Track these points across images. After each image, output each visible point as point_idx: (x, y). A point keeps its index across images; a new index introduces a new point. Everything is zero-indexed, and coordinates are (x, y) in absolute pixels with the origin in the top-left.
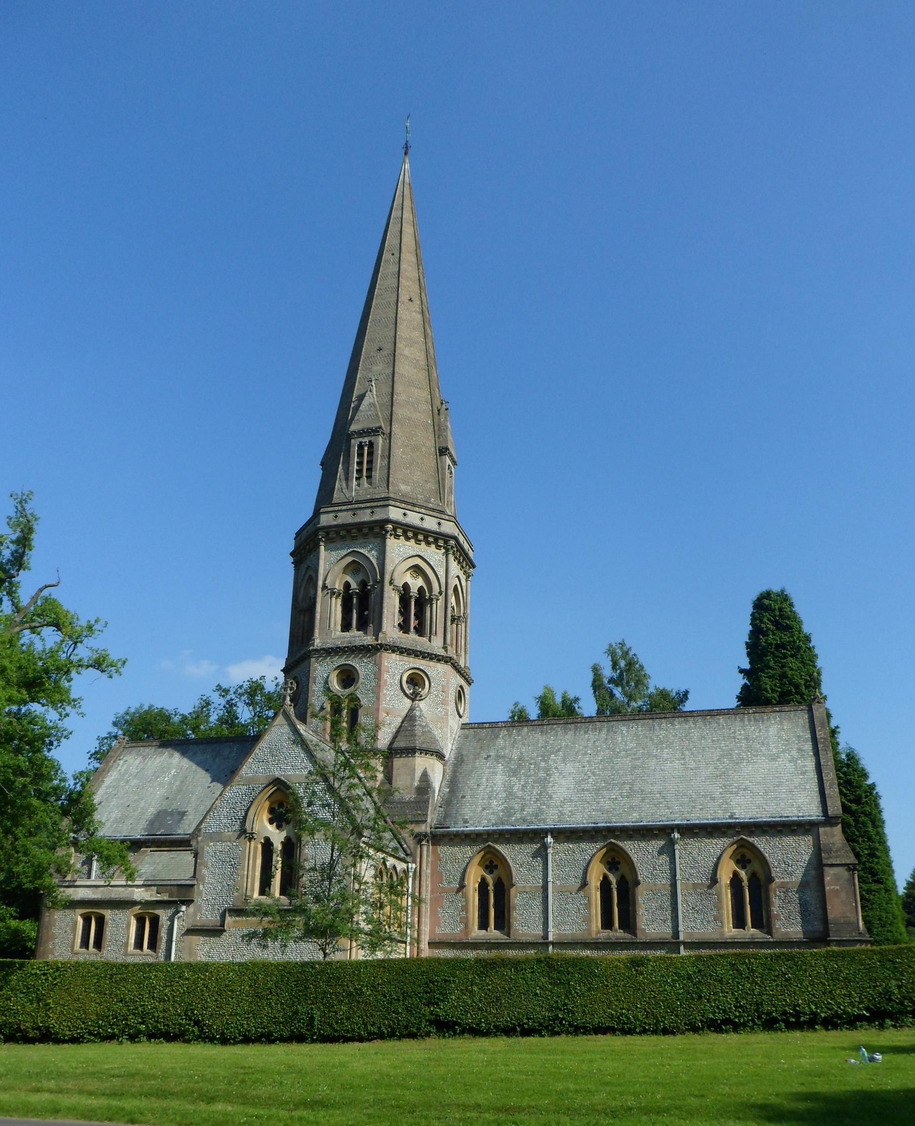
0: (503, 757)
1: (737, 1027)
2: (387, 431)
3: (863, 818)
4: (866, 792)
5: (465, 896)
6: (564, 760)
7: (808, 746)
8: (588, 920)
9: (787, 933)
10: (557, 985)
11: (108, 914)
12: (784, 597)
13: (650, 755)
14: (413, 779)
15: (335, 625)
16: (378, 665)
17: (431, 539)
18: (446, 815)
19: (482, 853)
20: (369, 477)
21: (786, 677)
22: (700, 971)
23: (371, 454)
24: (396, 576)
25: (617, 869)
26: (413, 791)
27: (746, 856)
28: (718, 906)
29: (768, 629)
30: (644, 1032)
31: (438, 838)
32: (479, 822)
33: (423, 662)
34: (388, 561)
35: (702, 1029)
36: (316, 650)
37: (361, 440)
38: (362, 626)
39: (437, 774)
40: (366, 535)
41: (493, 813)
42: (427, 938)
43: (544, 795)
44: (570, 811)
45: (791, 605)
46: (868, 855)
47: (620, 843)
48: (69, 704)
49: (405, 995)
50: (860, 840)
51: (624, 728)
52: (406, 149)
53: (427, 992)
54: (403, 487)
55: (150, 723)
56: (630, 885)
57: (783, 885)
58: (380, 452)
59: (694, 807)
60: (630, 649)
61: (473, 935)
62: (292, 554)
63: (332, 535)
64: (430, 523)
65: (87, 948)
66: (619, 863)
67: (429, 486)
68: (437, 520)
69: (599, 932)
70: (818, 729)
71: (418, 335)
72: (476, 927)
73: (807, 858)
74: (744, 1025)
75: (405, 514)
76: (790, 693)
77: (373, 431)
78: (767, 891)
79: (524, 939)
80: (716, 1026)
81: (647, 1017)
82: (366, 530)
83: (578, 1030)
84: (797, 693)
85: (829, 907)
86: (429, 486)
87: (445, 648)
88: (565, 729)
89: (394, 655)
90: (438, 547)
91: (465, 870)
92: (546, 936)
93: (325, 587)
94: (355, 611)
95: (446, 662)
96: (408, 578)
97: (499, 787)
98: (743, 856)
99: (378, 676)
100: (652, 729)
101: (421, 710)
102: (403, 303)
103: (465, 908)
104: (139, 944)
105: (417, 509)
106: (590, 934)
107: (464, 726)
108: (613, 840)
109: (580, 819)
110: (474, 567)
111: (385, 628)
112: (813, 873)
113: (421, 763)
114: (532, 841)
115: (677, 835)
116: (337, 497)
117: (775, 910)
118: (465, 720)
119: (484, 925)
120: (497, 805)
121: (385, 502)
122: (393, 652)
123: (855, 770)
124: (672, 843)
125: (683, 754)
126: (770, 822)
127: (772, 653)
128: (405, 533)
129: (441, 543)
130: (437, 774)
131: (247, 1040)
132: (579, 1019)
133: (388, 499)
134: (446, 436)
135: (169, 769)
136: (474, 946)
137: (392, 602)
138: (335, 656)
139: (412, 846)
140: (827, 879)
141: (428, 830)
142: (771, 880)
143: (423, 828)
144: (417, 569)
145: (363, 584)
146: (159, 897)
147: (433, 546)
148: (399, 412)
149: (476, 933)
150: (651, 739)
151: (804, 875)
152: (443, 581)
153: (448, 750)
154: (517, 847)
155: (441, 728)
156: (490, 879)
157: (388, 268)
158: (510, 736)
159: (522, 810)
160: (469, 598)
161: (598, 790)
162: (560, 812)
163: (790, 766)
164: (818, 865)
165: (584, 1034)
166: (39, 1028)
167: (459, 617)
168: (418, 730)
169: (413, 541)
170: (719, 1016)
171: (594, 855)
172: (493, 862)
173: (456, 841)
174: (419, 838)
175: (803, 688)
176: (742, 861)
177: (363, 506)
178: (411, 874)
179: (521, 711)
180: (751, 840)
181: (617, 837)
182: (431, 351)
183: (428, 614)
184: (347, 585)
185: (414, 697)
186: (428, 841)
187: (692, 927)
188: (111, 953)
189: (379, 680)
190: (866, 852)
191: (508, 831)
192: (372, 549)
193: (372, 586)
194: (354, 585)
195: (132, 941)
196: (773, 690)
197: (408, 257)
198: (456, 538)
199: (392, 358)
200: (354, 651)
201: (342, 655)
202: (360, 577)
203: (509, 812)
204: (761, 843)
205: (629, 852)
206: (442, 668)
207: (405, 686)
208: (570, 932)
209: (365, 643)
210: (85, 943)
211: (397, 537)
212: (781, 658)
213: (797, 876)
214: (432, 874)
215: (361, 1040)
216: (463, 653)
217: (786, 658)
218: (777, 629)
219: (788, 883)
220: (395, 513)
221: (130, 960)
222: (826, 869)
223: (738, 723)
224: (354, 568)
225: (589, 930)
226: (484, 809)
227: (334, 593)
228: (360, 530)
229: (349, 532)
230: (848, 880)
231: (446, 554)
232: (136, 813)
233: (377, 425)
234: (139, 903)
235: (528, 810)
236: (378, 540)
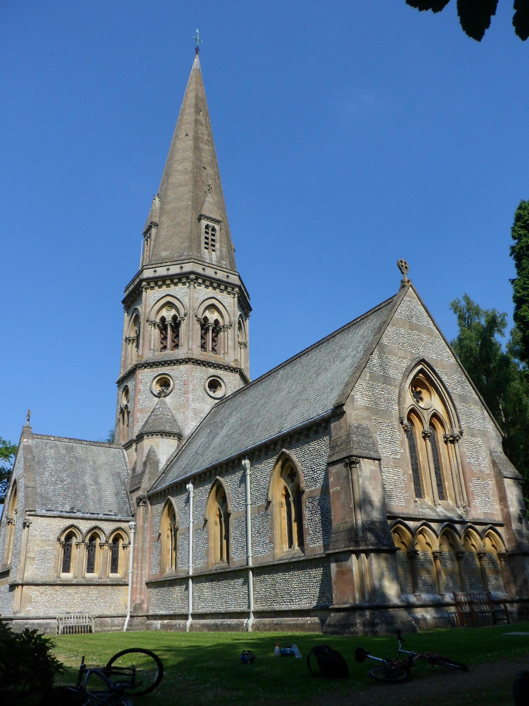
17: (176, 281)
54: (164, 254)
64: (175, 270)
68: (179, 266)
71: (190, 154)
89: (146, 370)
90: (184, 284)
95: (187, 362)
122: (145, 367)
129: (184, 280)
143: (140, 493)
144: (169, 305)
155: (183, 413)
174: (139, 500)
178: (133, 531)
186: (144, 502)
198: (192, 273)
206: (183, 368)
207: (157, 389)
211: (152, 288)
230: (347, 476)
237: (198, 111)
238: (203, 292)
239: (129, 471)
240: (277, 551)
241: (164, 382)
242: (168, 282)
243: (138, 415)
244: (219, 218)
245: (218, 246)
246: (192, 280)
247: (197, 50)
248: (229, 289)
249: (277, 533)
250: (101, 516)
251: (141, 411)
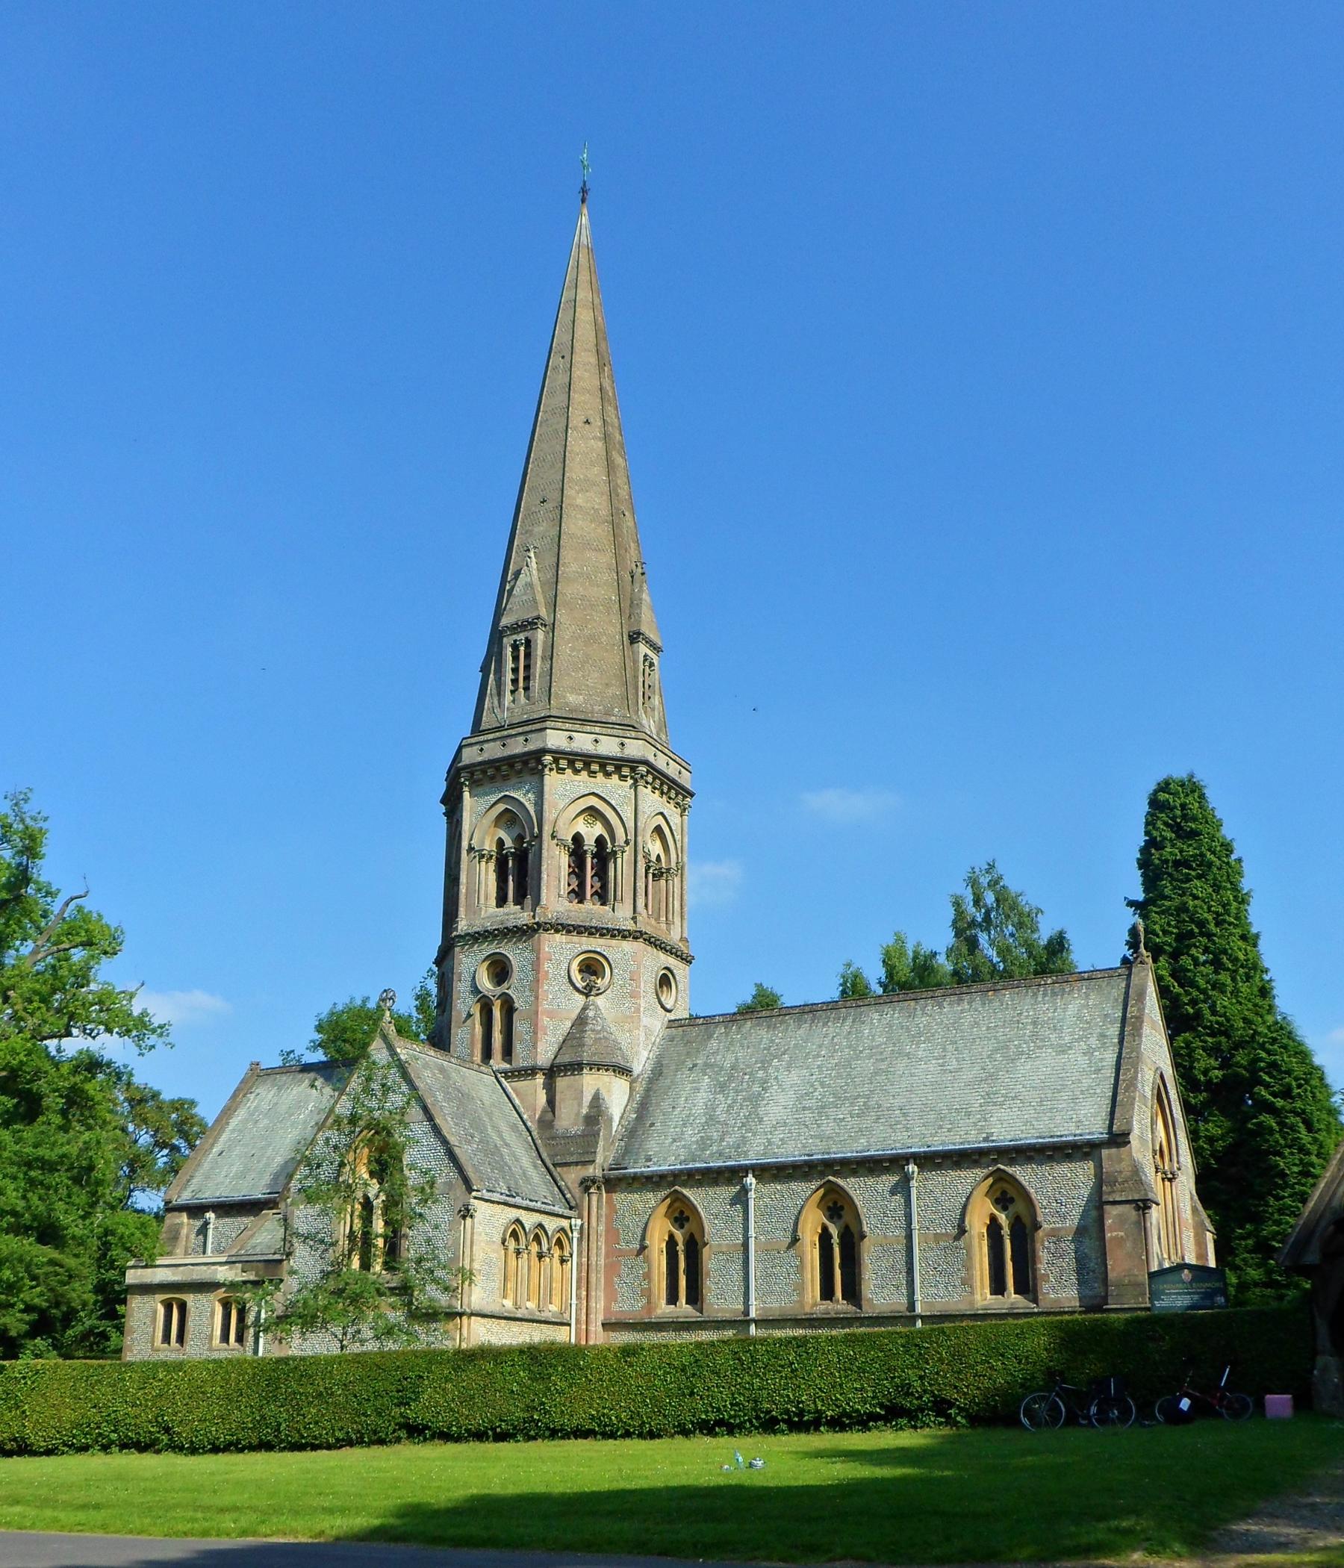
0: (712, 1066)
1: (731, 1429)
2: (549, 620)
3: (1292, 1119)
4: (1296, 1079)
5: (647, 1260)
6: (788, 1068)
7: (1114, 1031)
8: (800, 1288)
9: (1057, 1300)
10: (537, 1380)
11: (190, 1299)
12: (1192, 787)
13: (901, 1053)
14: (580, 1105)
15: (486, 898)
16: (537, 951)
17: (610, 768)
18: (627, 1151)
19: (668, 1201)
20: (526, 689)
21: (1187, 910)
22: (696, 1361)
23: (528, 655)
24: (560, 823)
25: (840, 1217)
26: (581, 1120)
27: (1007, 1193)
28: (968, 1267)
29: (1164, 838)
30: (628, 1435)
31: (614, 1183)
32: (665, 1159)
33: (601, 941)
34: (546, 807)
35: (694, 1433)
36: (460, 936)
37: (515, 637)
38: (519, 900)
39: (617, 1096)
40: (520, 772)
41: (684, 1147)
42: (601, 1318)
43: (754, 1117)
44: (781, 1140)
45: (1202, 796)
46: (1300, 1173)
47: (840, 1181)
48: (154, 1031)
49: (377, 1395)
50: (1287, 1151)
51: (876, 1016)
52: (584, 191)
53: (398, 1391)
54: (571, 698)
55: (344, 1030)
56: (856, 1239)
57: (1054, 1233)
58: (539, 652)
59: (941, 1127)
60: (1001, 878)
61: (659, 1312)
62: (442, 802)
63: (478, 775)
64: (608, 746)
65: (227, 1342)
66: (842, 1208)
67: (610, 691)
69: (815, 1305)
70: (1131, 1002)
71: (598, 473)
72: (663, 1302)
73: (1085, 1192)
74: (740, 1427)
75: (571, 738)
76: (1191, 934)
77: (530, 623)
78: (1033, 1241)
79: (720, 1316)
80: (708, 1428)
81: (632, 1418)
82: (518, 766)
83: (554, 1433)
84: (1202, 934)
85: (1109, 1263)
86: (610, 691)
87: (634, 918)
88: (799, 1020)
89: (558, 936)
90: (623, 778)
91: (646, 1224)
92: (746, 1313)
93: (471, 849)
94: (511, 878)
95: (635, 938)
96: (581, 827)
97: (699, 1110)
98: (1004, 1193)
99: (536, 965)
100: (912, 1015)
101: (597, 1008)
102: (575, 428)
103: (647, 1276)
104: (225, 1337)
105: (588, 729)
106: (802, 1306)
107: (672, 1024)
108: (831, 1178)
109: (791, 1152)
110: (692, 795)
111: (544, 901)
112: (1094, 1213)
113: (590, 1082)
114: (729, 1182)
115: (912, 1168)
116: (487, 721)
117: (1042, 1268)
118: (672, 1016)
119: (672, 1299)
120: (691, 1135)
121: (538, 724)
122: (557, 931)
123: (1285, 1047)
124: (907, 1179)
125: (944, 1050)
126: (1035, 1144)
127: (1170, 875)
128: (571, 764)
129: (626, 771)
130: (617, 1096)
131: (216, 1449)
132: (558, 1421)
133: (543, 719)
134: (639, 615)
135: (307, 1102)
136: (659, 1326)
137: (555, 864)
138: (483, 943)
139: (577, 1195)
140: (1108, 1222)
141: (599, 1173)
142: (1037, 1226)
143: (591, 1171)
144: (593, 812)
145: (519, 839)
146: (245, 1277)
147: (615, 777)
148: (566, 590)
149: (663, 1309)
150: (908, 1030)
151: (1083, 1217)
152: (630, 825)
153: (641, 1063)
154: (711, 1191)
155: (630, 1031)
156: (679, 1236)
157: (557, 380)
158: (727, 1034)
159: (722, 1140)
160: (686, 840)
161: (823, 1107)
162: (769, 1141)
163: (1083, 1061)
164: (1098, 1204)
165: (562, 1438)
166: (15, 1439)
167: (668, 870)
168: (589, 1037)
169: (584, 773)
170: (712, 1416)
171: (807, 1199)
172: (683, 1215)
173: (636, 1185)
174: (586, 1184)
175: (1212, 926)
176: (1003, 1201)
177: (513, 732)
178: (576, 1235)
179: (856, 976)
180: (1010, 1170)
181: (835, 1174)
182: (623, 493)
183: (611, 873)
184: (500, 843)
185: (587, 991)
186: (599, 1188)
187: (932, 1296)
188: (195, 1350)
189: (538, 972)
190: (1296, 1169)
191: (698, 1170)
192: (528, 791)
193: (529, 843)
194: (509, 843)
195: (218, 1332)
196: (1165, 932)
197: (585, 359)
198: (646, 763)
199: (558, 512)
200: (505, 935)
201: (492, 941)
202: (516, 831)
203: (704, 1143)
204: (1023, 1174)
205: (851, 1193)
206: (628, 946)
207: (577, 977)
208: (777, 1305)
209: (519, 923)
210: (166, 1338)
211: (561, 770)
212: (1182, 882)
213: (1072, 1222)
214: (607, 1231)
215: (329, 1447)
216: (677, 920)
217: (1188, 880)
218: (1179, 837)
219: (1059, 1229)
220: (555, 739)
221: (216, 1355)
222: (1107, 1208)
223: (1028, 1000)
224: (509, 818)
225: (801, 1303)
226: (674, 1140)
227: (483, 856)
228: (512, 766)
229: (498, 769)
231: (635, 786)
232: (261, 1165)
233: (535, 614)
234: (223, 1285)
235: (730, 1140)
236: (536, 777)
237: (601, 366)
238: (652, 800)
239: (529, 1124)
240: (978, 1297)
241: (591, 967)
242: (595, 767)
243: (544, 1021)
244: (660, 644)
245: (656, 700)
248: (673, 795)
249: (977, 1273)
250: (539, 1205)
251: (551, 1015)
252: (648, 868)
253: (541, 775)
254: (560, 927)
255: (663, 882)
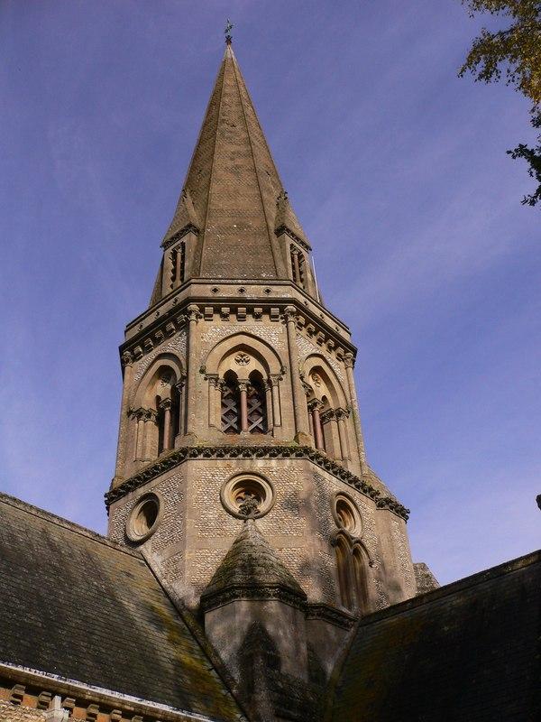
2: (198, 223)
90: (274, 318)
96: (231, 364)
160: (354, 391)
211: (209, 317)
246: (292, 313)
247: (229, 40)
252: (311, 409)
253: (185, 326)
254: (208, 453)
255: (334, 424)
